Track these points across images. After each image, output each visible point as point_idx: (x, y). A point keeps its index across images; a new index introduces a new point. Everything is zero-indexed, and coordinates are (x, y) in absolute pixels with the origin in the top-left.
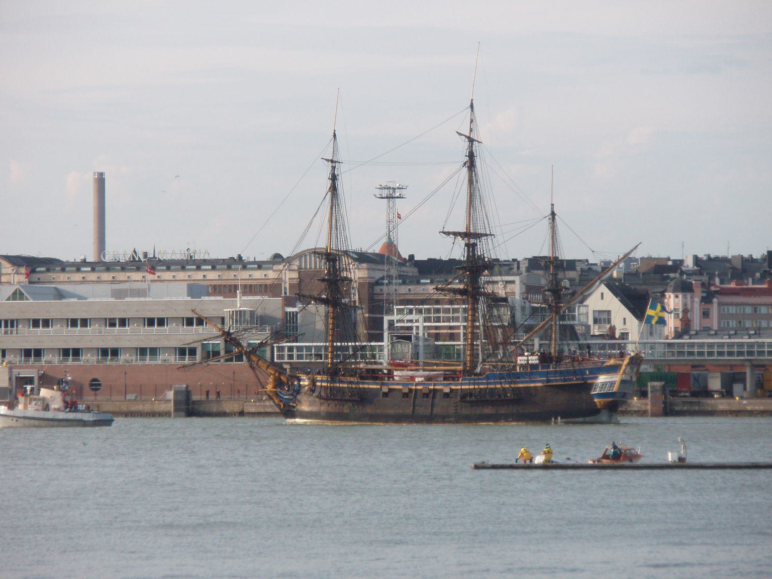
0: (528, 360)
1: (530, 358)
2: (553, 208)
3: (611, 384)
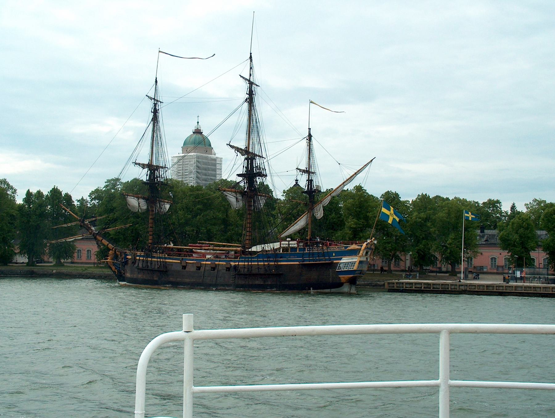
0: (289, 244)
1: (290, 242)
2: (310, 132)
3: (352, 264)
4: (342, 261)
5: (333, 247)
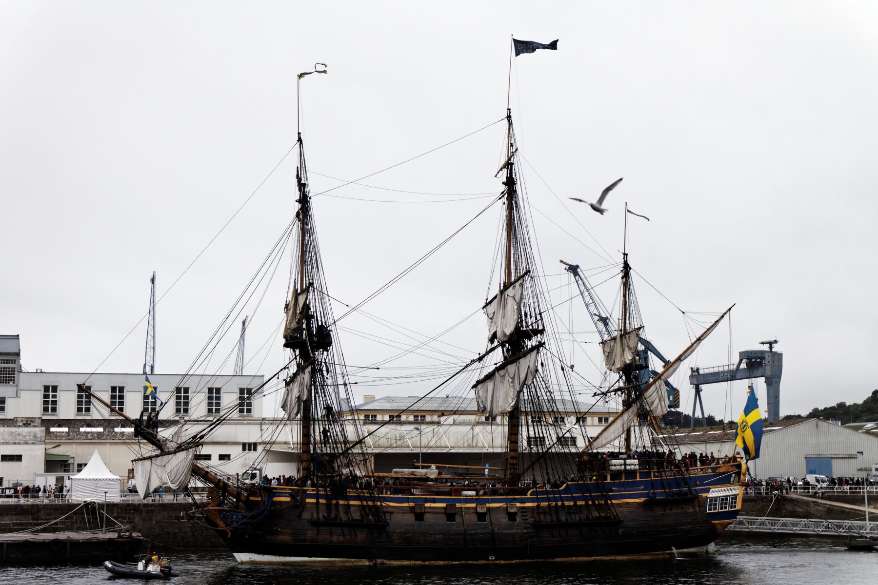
0: (625, 465)
1: (628, 461)
4: (711, 494)
5: (694, 469)
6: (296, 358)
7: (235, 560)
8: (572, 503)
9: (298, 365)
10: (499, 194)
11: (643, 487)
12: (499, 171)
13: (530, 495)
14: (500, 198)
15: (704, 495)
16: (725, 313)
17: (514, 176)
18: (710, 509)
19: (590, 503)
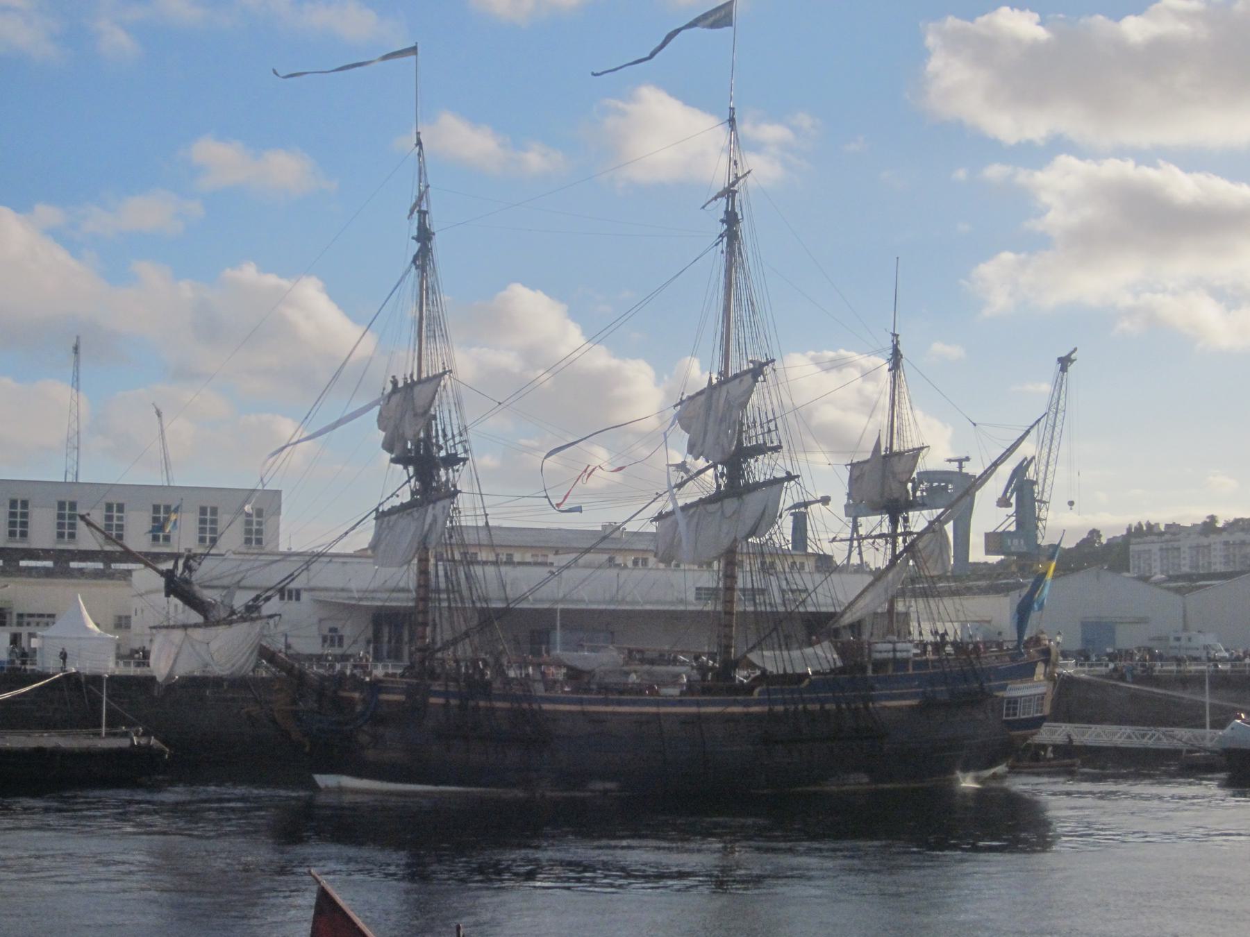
0: (895, 650)
3: (1038, 699)
6: (409, 481)
7: (315, 787)
8: (818, 707)
9: (413, 493)
10: (715, 238)
11: (917, 683)
12: (712, 200)
13: (759, 695)
14: (717, 244)
15: (1001, 694)
16: (1032, 427)
17: (737, 210)
18: (1007, 715)
19: (844, 706)
